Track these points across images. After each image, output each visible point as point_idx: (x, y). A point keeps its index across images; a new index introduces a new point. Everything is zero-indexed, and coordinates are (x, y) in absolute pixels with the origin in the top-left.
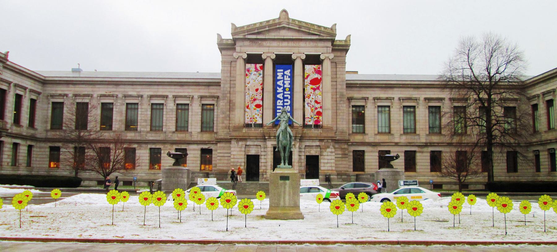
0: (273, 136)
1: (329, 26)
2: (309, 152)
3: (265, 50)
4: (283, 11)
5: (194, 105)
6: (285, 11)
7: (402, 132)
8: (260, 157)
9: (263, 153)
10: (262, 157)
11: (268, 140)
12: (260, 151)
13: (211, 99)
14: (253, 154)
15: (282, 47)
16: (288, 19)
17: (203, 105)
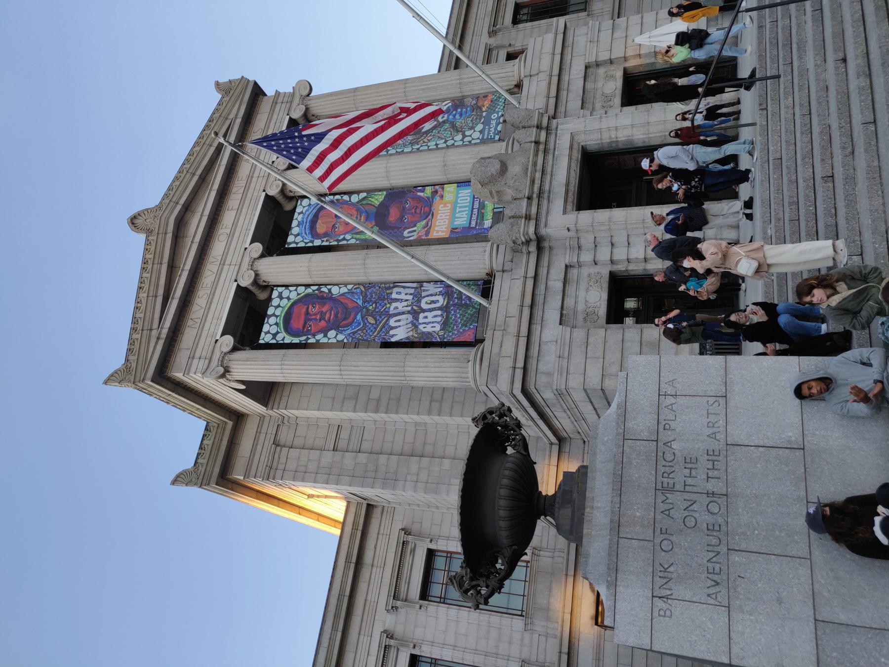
0: (529, 205)
1: (216, 97)
2: (608, 98)
3: (229, 273)
4: (133, 224)
5: (418, 634)
6: (133, 221)
7: (584, 14)
8: (620, 267)
9: (604, 255)
10: (620, 254)
11: (542, 224)
12: (593, 270)
13: (408, 559)
14: (605, 296)
15: (235, 224)
16: (159, 207)
17: (424, 595)
